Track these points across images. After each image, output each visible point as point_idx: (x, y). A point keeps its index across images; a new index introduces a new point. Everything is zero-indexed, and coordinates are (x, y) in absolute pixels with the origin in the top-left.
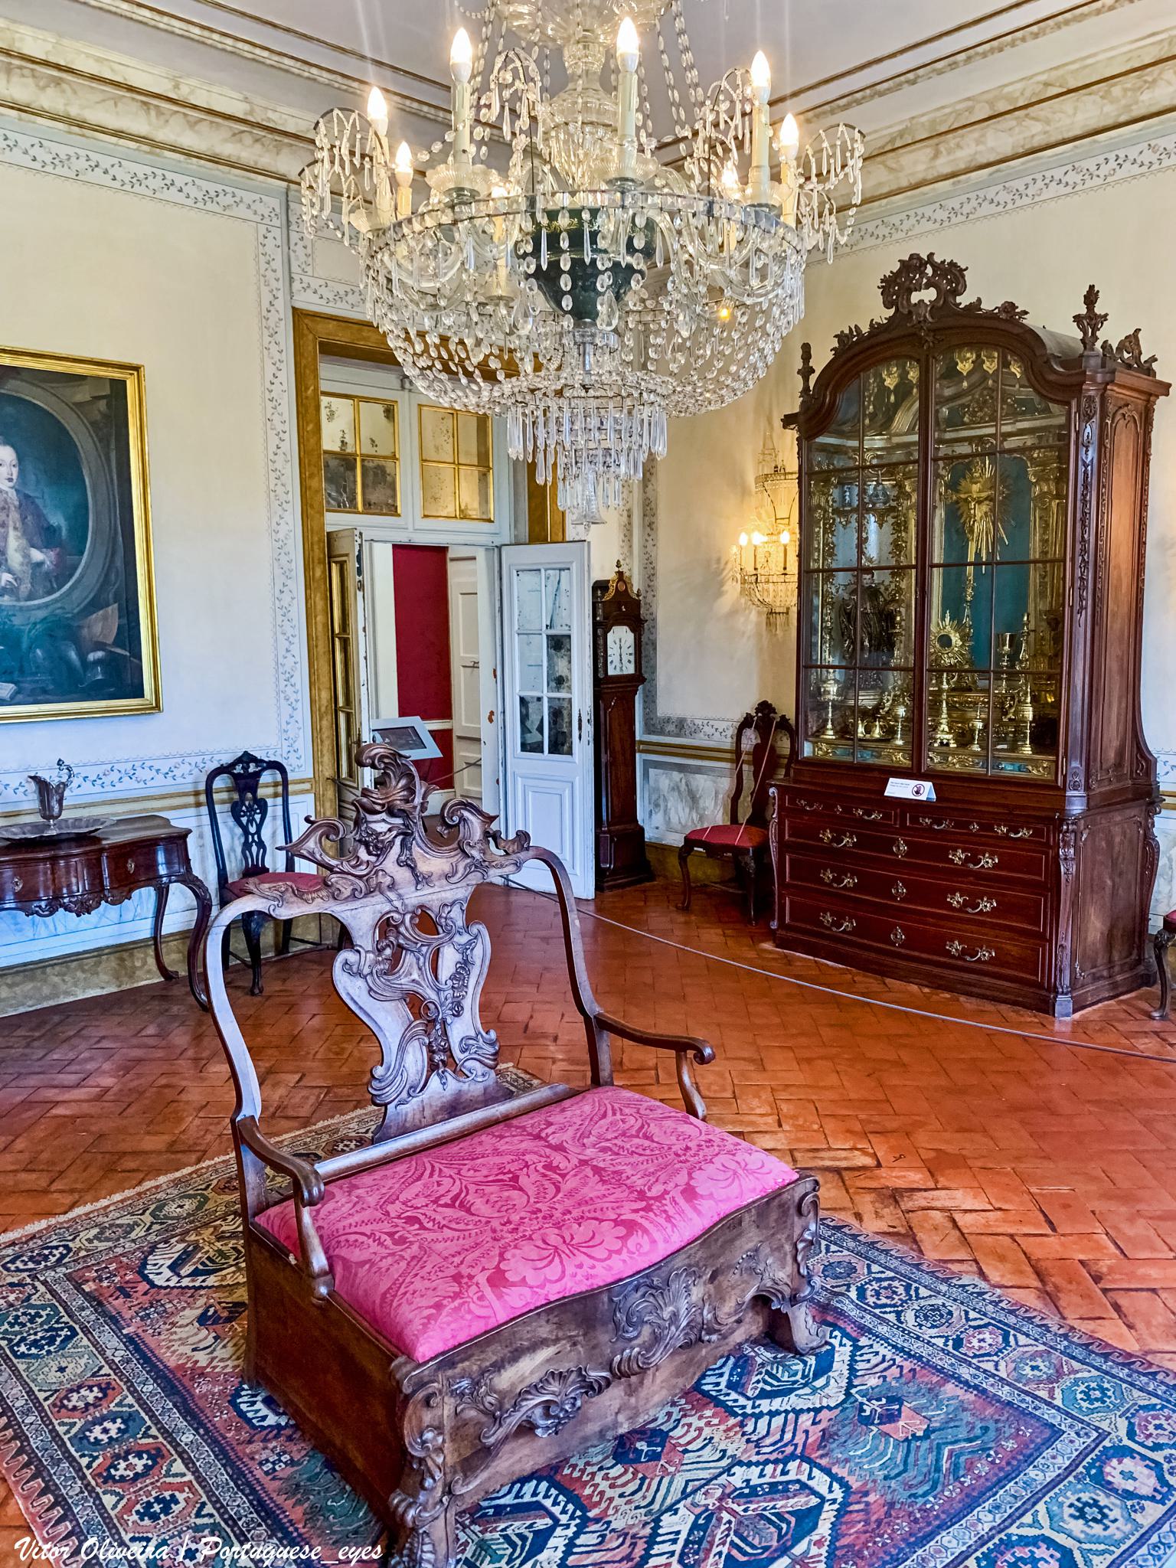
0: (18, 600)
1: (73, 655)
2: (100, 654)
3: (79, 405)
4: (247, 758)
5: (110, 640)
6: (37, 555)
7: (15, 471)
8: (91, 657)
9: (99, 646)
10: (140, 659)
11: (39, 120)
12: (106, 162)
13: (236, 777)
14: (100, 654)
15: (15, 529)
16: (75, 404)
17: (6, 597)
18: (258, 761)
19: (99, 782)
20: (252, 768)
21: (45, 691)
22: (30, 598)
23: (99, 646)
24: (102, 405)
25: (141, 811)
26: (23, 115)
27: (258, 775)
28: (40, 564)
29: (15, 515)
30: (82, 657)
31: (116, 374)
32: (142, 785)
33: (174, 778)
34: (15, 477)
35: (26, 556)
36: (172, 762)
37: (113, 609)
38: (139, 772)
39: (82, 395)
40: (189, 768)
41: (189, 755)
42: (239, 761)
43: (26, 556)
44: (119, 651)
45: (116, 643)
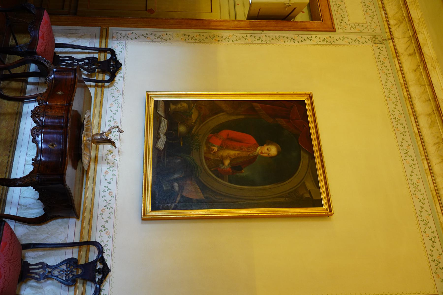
0: (205, 153)
1: (176, 176)
2: (177, 188)
3: (304, 185)
4: (106, 271)
5: (184, 194)
6: (227, 162)
7: (267, 155)
8: (176, 185)
9: (181, 188)
10: (174, 209)
11: (430, 177)
12: (426, 207)
13: (94, 263)
14: (177, 188)
15: (238, 154)
16: (304, 183)
17: (205, 148)
18: (101, 282)
19: (106, 189)
20: (98, 277)
21: (159, 162)
22: (206, 159)
23: (181, 188)
24: (307, 195)
25: (84, 210)
26: (428, 171)
27: (93, 280)
28: (223, 164)
29: (245, 153)
30: (176, 180)
31: (324, 203)
32: (100, 212)
33: (101, 231)
34: (263, 155)
35: (226, 158)
36: (110, 230)
37: (201, 196)
38: (108, 211)
39: (310, 185)
40: (105, 241)
41: (113, 241)
42: (105, 265)
43: (226, 158)
44: (178, 199)
45: (182, 197)
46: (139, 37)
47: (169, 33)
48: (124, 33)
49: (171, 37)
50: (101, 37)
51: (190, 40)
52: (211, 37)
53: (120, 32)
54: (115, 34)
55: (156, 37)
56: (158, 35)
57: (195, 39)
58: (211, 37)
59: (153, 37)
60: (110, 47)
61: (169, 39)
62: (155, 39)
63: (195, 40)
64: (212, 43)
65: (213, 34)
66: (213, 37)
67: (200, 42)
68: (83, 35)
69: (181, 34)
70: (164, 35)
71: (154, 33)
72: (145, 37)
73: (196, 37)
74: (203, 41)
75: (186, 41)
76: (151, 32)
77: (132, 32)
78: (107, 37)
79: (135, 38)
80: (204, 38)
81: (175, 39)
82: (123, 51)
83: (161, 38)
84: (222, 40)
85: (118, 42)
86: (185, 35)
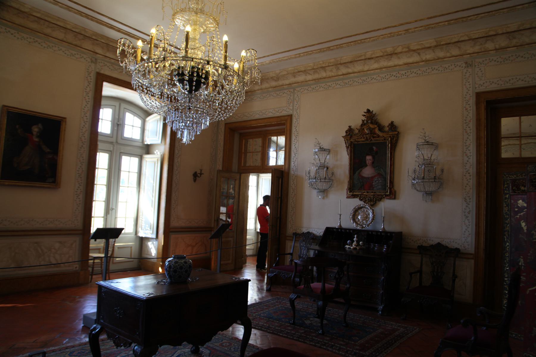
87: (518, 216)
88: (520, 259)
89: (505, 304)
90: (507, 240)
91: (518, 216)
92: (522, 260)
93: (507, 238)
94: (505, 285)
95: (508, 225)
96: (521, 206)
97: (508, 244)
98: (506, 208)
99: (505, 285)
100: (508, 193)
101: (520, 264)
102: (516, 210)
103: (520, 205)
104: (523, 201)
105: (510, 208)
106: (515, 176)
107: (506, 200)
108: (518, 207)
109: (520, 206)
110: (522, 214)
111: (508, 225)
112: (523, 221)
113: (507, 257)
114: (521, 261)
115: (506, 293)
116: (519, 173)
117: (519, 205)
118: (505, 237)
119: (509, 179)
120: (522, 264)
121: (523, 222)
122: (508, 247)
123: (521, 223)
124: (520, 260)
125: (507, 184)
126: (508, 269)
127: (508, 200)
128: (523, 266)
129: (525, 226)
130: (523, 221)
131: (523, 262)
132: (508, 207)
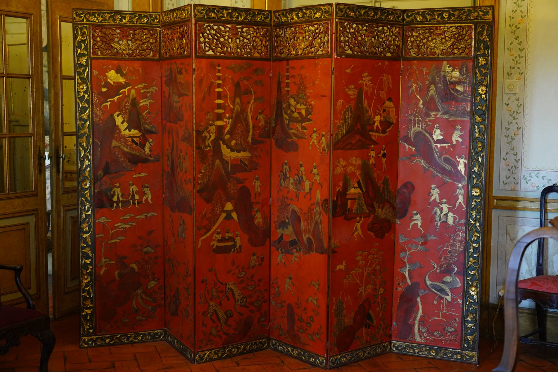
46: (513, 149)
47: (505, 101)
48: (504, 173)
49: (513, 98)
50: (515, 209)
51: (521, 66)
52: (515, 31)
53: (503, 178)
54: (506, 187)
55: (514, 121)
56: (510, 119)
57: (518, 57)
58: (515, 31)
59: (513, 127)
60: (538, 195)
61: (518, 100)
62: (517, 123)
63: (520, 57)
64: (527, 29)
65: (508, 27)
66: (514, 26)
67: (524, 49)
68: (510, 236)
69: (507, 82)
70: (510, 109)
71: (505, 124)
72: (513, 139)
73: (515, 56)
74: (524, 43)
75: (522, 73)
76: (504, 129)
77: (502, 159)
78: (515, 200)
79: (516, 154)
80: (516, 42)
81: (517, 90)
82: (542, 174)
83: (515, 113)
84: (521, 11)
85: (523, 182)
86: (509, 74)
87: (108, 104)
88: (115, 189)
89: (86, 286)
90: (84, 155)
91: (108, 104)
92: (118, 191)
93: (85, 150)
94: (84, 248)
95: (88, 123)
96: (114, 82)
97: (87, 162)
98: (81, 87)
99: (84, 248)
100: (84, 55)
101: (115, 199)
102: (104, 90)
103: (111, 80)
104: (117, 72)
105: (89, 86)
106: (100, 19)
107: (81, 70)
108: (107, 85)
109: (112, 83)
110: (115, 98)
111: (88, 123)
112: (118, 113)
113: (86, 189)
114: (116, 194)
115: (88, 263)
116: (108, 13)
117: (109, 80)
118: (81, 149)
119: (87, 24)
120: (118, 198)
121: (118, 116)
122: (89, 169)
123: (115, 117)
124: (114, 192)
125: (83, 34)
126: (89, 213)
127: (86, 69)
128: (122, 202)
129: (122, 123)
130: (118, 113)
131: (120, 194)
132: (87, 85)
